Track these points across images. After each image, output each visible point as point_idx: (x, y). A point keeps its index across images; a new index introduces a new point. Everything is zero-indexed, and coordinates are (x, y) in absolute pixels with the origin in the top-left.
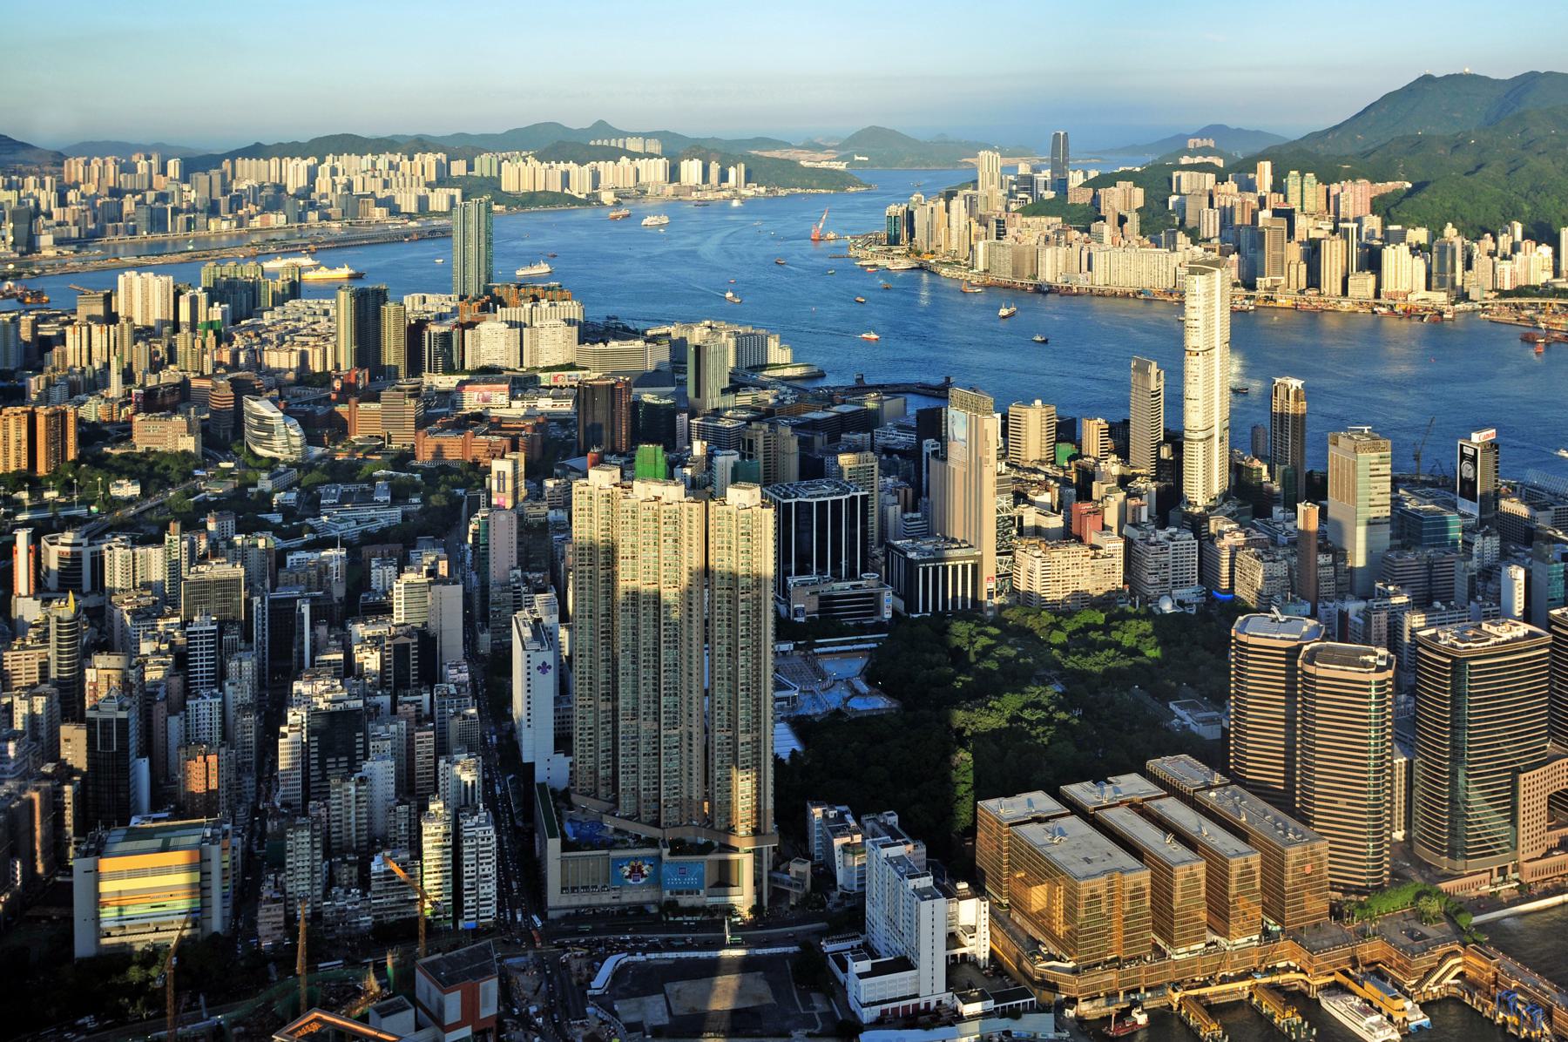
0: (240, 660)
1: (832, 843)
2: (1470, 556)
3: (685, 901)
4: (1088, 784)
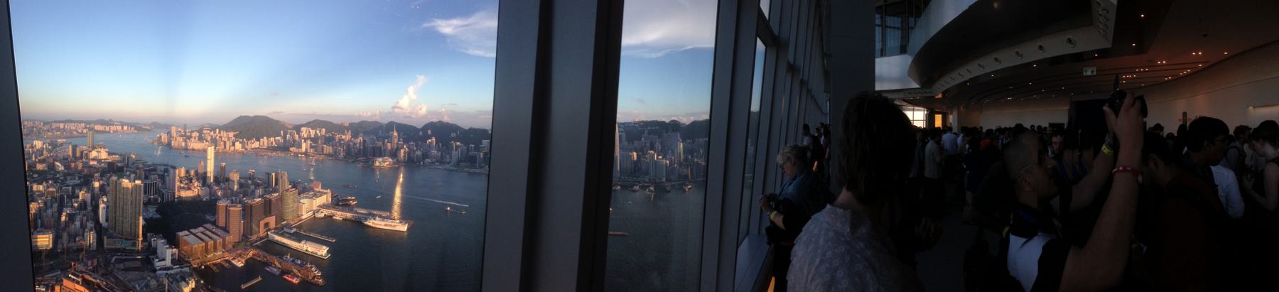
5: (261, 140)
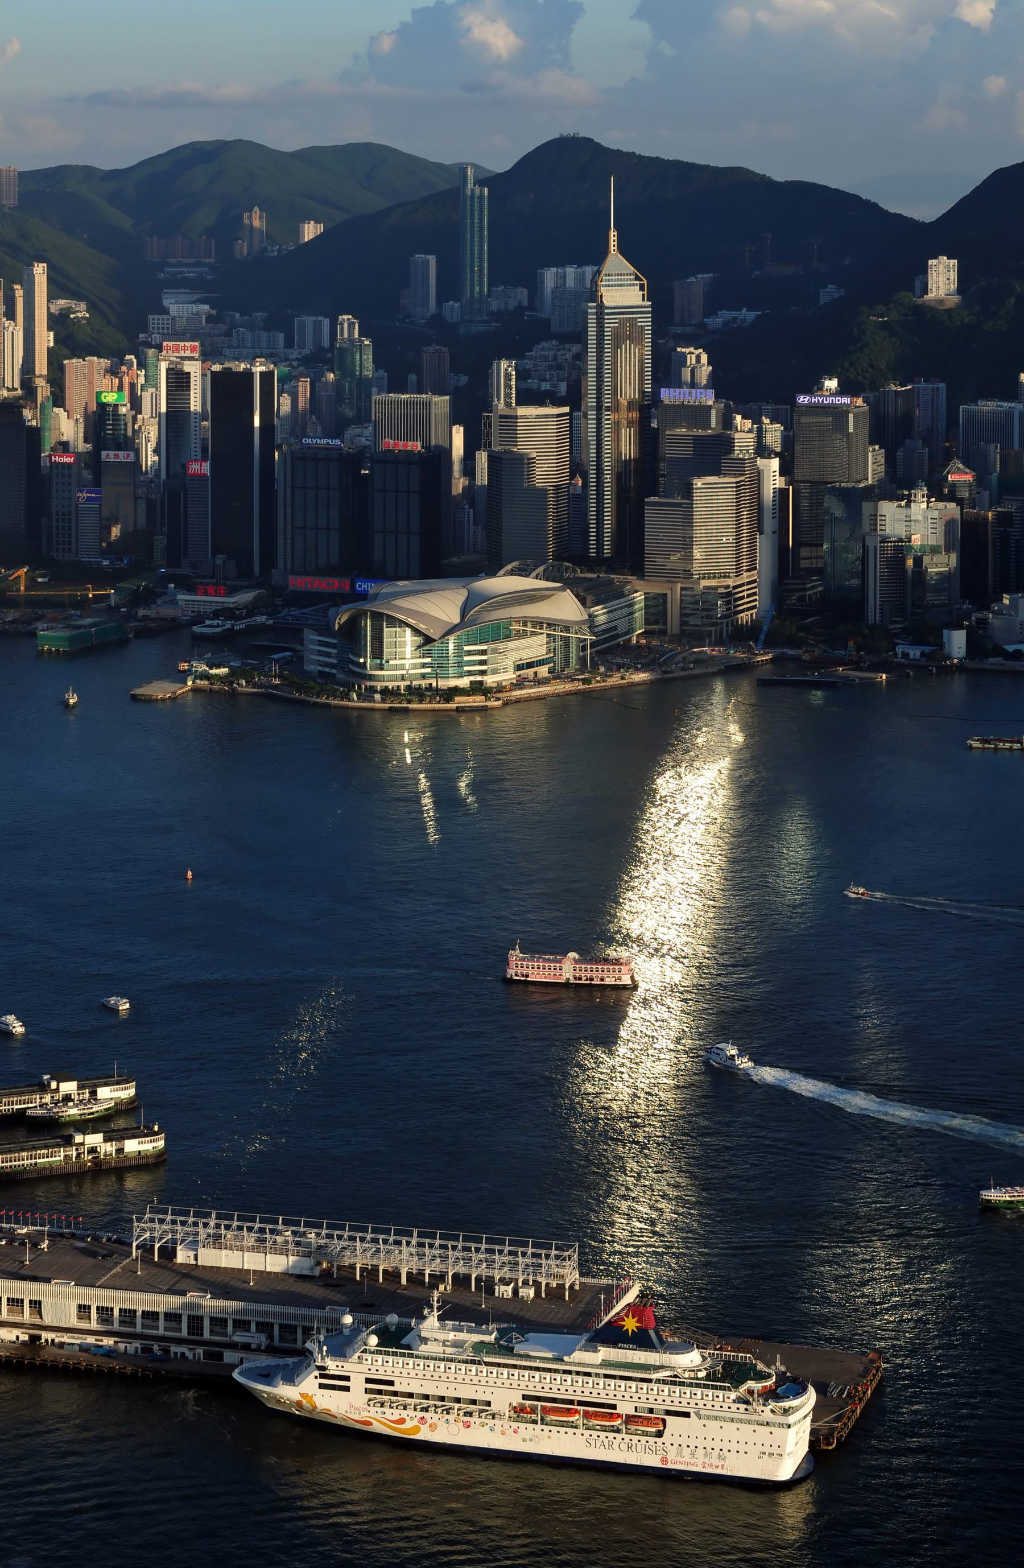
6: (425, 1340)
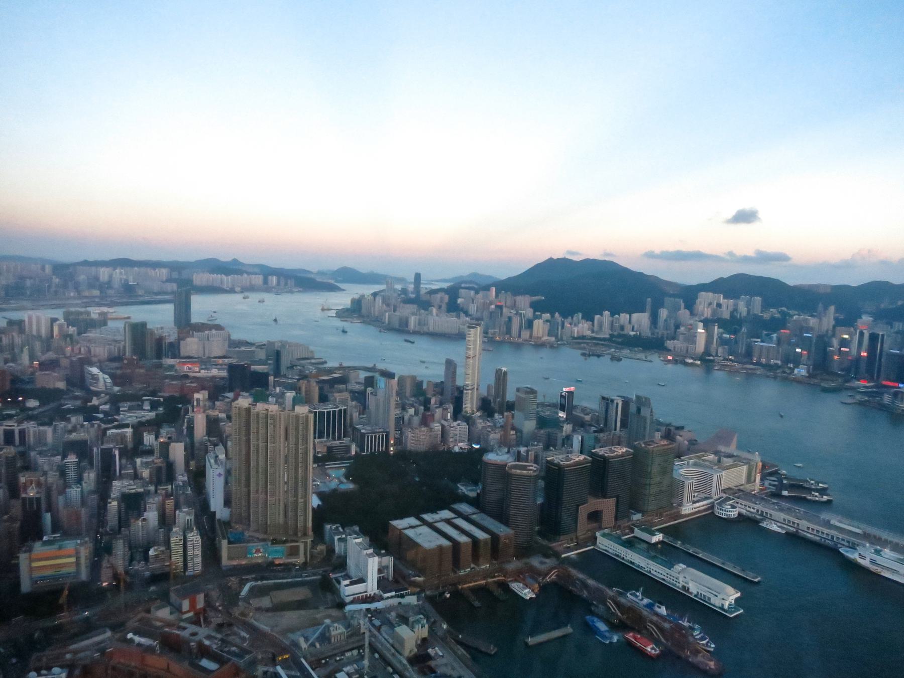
0: (89, 473)
1: (334, 539)
2: (562, 432)
3: (277, 562)
4: (430, 515)
5: (597, 317)
6: (886, 554)
